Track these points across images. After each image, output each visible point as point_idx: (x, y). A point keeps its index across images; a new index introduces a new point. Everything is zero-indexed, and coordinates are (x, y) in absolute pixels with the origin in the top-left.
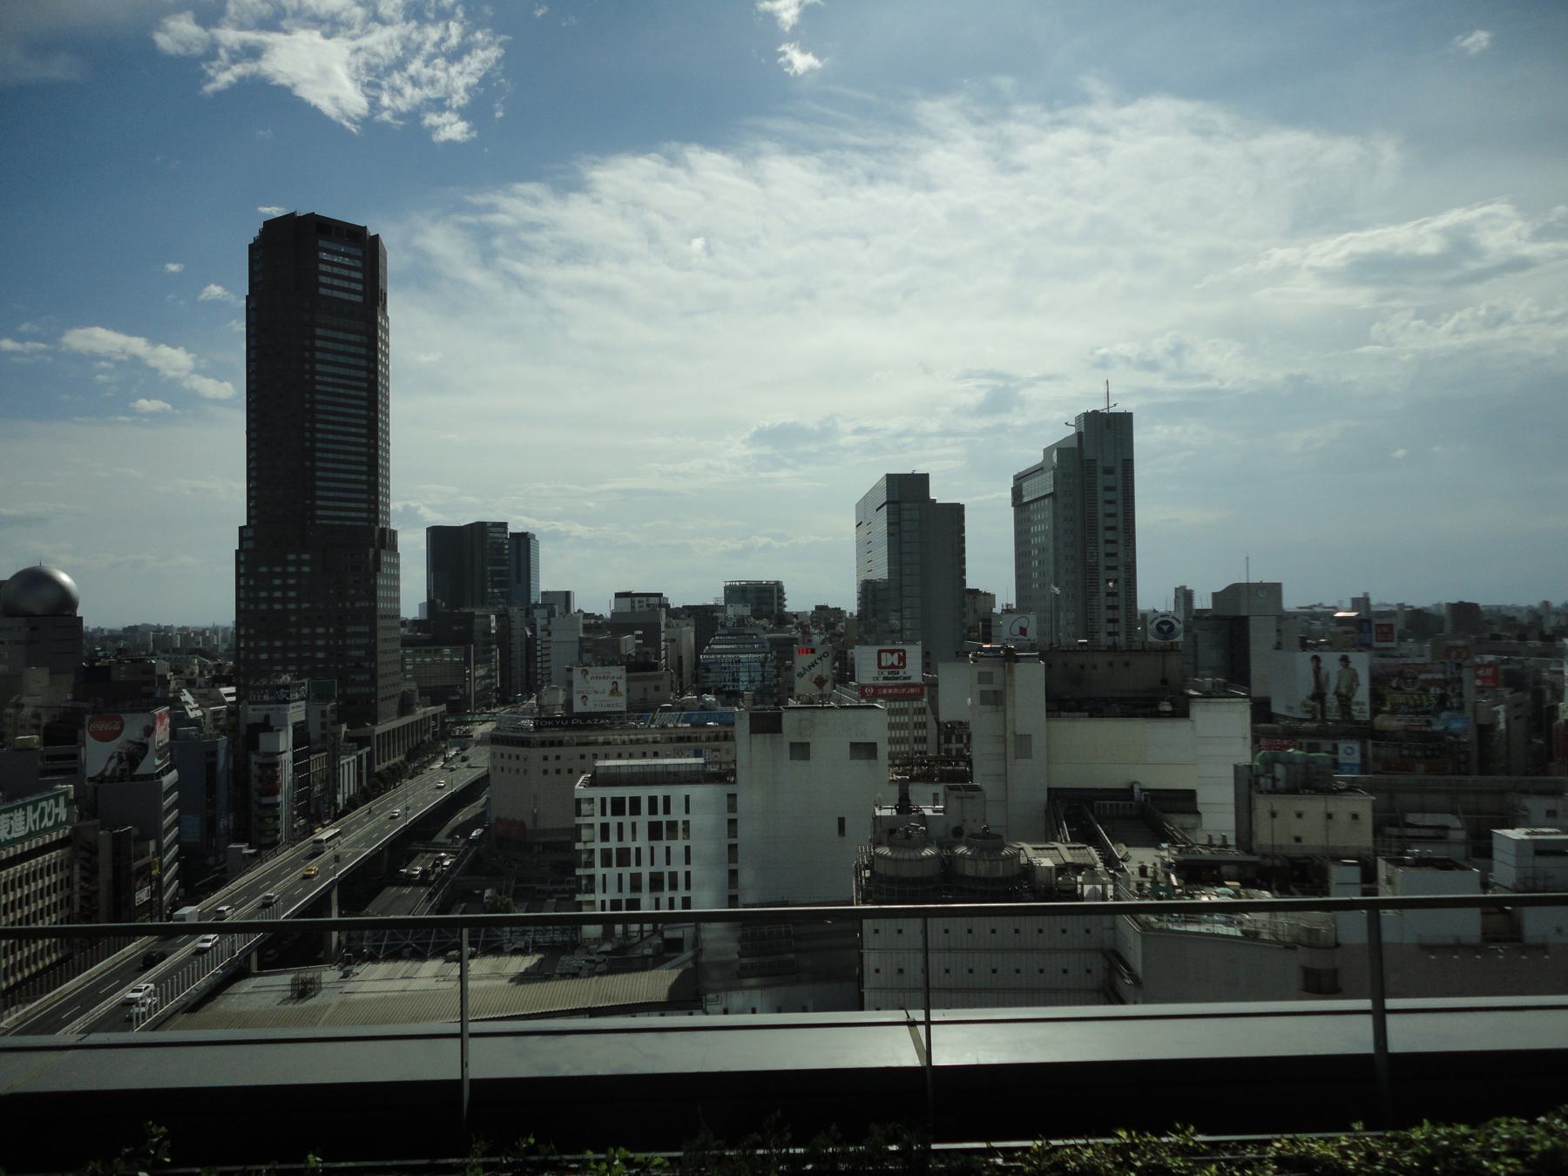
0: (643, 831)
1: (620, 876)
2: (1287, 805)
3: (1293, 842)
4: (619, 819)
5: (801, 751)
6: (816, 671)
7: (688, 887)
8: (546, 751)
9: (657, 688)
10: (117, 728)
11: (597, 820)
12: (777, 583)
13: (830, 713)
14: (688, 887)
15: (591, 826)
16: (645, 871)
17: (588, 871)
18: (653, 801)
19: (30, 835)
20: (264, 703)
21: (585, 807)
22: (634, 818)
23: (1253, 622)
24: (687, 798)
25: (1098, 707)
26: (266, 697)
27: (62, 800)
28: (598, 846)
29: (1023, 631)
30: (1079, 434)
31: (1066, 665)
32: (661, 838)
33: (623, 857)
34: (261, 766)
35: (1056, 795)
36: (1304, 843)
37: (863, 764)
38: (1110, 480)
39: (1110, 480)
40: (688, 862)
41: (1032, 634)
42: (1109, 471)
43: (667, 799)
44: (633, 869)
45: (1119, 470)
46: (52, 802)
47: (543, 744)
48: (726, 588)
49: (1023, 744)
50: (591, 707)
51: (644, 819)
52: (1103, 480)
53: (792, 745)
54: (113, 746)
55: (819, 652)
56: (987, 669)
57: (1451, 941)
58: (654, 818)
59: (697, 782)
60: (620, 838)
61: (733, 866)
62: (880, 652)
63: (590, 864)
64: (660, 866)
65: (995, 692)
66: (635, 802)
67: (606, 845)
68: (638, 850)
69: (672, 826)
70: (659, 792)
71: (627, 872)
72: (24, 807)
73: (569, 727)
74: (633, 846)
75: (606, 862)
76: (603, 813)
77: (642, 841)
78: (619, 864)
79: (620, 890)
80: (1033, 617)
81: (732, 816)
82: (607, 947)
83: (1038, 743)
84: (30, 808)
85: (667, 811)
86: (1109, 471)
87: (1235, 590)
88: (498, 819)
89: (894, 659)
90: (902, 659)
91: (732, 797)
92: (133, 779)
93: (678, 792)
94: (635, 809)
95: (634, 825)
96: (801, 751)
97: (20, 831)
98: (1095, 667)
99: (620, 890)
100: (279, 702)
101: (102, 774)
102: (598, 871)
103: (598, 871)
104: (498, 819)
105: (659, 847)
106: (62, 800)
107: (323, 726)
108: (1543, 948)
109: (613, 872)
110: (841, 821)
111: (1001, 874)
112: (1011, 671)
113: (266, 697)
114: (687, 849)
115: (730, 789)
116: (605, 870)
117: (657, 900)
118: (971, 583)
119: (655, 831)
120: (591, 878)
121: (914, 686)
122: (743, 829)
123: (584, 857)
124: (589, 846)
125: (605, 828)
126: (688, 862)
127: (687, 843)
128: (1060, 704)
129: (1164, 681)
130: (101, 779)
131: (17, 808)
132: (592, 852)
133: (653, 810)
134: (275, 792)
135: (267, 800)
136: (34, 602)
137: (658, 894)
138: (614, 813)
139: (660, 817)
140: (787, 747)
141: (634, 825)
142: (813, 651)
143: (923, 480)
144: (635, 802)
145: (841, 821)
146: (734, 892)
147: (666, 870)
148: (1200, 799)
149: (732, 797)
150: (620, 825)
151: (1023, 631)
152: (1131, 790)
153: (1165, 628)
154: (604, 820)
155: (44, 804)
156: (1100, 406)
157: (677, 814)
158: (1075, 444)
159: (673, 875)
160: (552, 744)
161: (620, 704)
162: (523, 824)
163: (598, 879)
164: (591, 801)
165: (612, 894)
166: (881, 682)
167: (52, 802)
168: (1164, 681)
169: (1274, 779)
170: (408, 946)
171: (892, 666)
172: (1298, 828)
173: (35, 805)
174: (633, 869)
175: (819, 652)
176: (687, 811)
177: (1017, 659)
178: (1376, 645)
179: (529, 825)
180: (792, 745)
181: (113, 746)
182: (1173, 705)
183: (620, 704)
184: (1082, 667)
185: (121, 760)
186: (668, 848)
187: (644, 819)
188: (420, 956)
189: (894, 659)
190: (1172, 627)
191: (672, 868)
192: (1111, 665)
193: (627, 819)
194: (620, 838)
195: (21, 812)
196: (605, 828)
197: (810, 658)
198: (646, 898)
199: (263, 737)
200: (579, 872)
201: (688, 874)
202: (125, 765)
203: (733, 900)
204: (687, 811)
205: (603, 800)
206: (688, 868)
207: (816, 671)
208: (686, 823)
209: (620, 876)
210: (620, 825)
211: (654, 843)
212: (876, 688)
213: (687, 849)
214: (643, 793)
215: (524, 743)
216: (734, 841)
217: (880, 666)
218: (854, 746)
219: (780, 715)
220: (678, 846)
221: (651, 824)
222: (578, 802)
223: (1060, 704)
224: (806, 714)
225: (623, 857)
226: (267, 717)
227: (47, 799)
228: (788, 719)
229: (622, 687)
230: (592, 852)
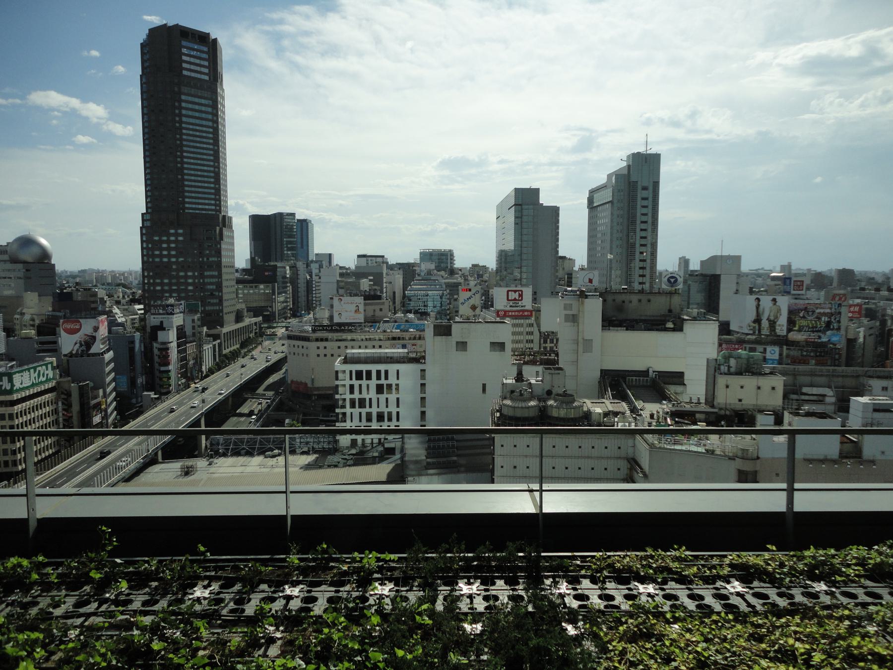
0: (373, 389)
1: (360, 413)
2: (736, 381)
3: (737, 402)
4: (360, 382)
5: (462, 346)
6: (472, 302)
7: (398, 420)
8: (319, 344)
9: (381, 310)
10: (77, 327)
11: (348, 382)
12: (450, 251)
13: (479, 325)
14: (398, 420)
15: (344, 386)
16: (374, 410)
17: (343, 410)
18: (378, 372)
19: (33, 385)
20: (160, 314)
21: (340, 375)
22: (369, 382)
23: (722, 277)
24: (398, 371)
25: (632, 325)
26: (161, 311)
27: (50, 366)
28: (348, 396)
29: (591, 281)
30: (629, 166)
31: (614, 300)
32: (383, 393)
33: (362, 403)
34: (159, 349)
35: (605, 373)
36: (743, 402)
37: (497, 354)
38: (645, 194)
39: (645, 194)
40: (398, 406)
41: (596, 283)
42: (645, 188)
43: (386, 372)
44: (368, 409)
45: (651, 188)
46: (44, 367)
47: (317, 340)
48: (421, 253)
49: (588, 344)
50: (343, 320)
51: (374, 382)
52: (641, 194)
54: (77, 337)
55: (473, 291)
56: (568, 302)
57: (822, 457)
58: (379, 382)
59: (404, 362)
60: (360, 393)
61: (423, 409)
62: (508, 291)
63: (344, 407)
64: (383, 408)
65: (573, 315)
66: (369, 373)
67: (352, 396)
68: (370, 399)
69: (389, 386)
70: (382, 367)
71: (364, 411)
72: (29, 370)
73: (332, 331)
74: (367, 397)
75: (353, 405)
76: (351, 379)
77: (373, 394)
78: (360, 407)
80: (596, 273)
81: (423, 382)
82: (353, 451)
83: (596, 345)
84: (32, 371)
85: (386, 378)
86: (645, 188)
87: (714, 260)
88: (292, 381)
89: (516, 295)
90: (521, 295)
91: (423, 371)
92: (89, 355)
93: (392, 368)
94: (369, 377)
95: (368, 386)
96: (462, 346)
97: (27, 383)
98: (631, 302)
99: (360, 421)
100: (168, 314)
101: (71, 353)
102: (348, 410)
103: (348, 410)
104: (292, 381)
105: (383, 397)
106: (50, 366)
107: (194, 328)
108: (873, 462)
109: (356, 411)
110: (484, 386)
112: (583, 303)
113: (161, 311)
114: (398, 399)
116: (352, 410)
118: (561, 253)
119: (380, 389)
120: (344, 414)
121: (527, 311)
122: (428, 388)
123: (340, 403)
124: (343, 397)
125: (352, 387)
126: (398, 406)
128: (610, 322)
129: (670, 311)
130: (71, 355)
131: (25, 370)
132: (344, 400)
133: (379, 378)
134: (167, 364)
135: (163, 369)
136: (28, 255)
138: (357, 379)
139: (383, 381)
141: (368, 386)
142: (470, 290)
143: (535, 192)
144: (369, 373)
145: (484, 386)
147: (386, 411)
148: (686, 377)
150: (360, 386)
151: (591, 281)
152: (648, 371)
153: (672, 280)
154: (351, 382)
155: (40, 368)
156: (641, 149)
157: (392, 380)
158: (626, 172)
159: (390, 414)
160: (322, 340)
161: (360, 318)
162: (306, 384)
163: (348, 415)
164: (344, 372)
166: (508, 308)
167: (44, 367)
168: (670, 311)
169: (729, 367)
170: (244, 449)
171: (515, 299)
172: (741, 394)
173: (35, 368)
174: (368, 409)
175: (473, 291)
176: (398, 378)
177: (586, 297)
178: (793, 292)
179: (310, 385)
181: (77, 337)
182: (674, 324)
183: (360, 318)
185: (81, 345)
186: (387, 399)
187: (374, 382)
188: (250, 454)
189: (516, 295)
190: (676, 280)
191: (389, 410)
192: (640, 301)
193: (364, 382)
194: (360, 393)
195: (27, 373)
196: (352, 387)
197: (468, 294)
199: (159, 333)
200: (337, 411)
201: (398, 413)
202: (84, 348)
204: (398, 378)
205: (351, 372)
206: (398, 410)
207: (472, 302)
208: (397, 385)
209: (360, 413)
210: (360, 386)
211: (379, 396)
212: (505, 312)
213: (398, 399)
214: (374, 368)
215: (306, 339)
216: (423, 395)
217: (508, 299)
218: (492, 344)
219: (451, 326)
220: (392, 397)
221: (377, 385)
222: (337, 372)
223: (610, 322)
225: (362, 403)
226: (162, 322)
227: (41, 366)
228: (455, 328)
229: (361, 308)
230: (344, 400)
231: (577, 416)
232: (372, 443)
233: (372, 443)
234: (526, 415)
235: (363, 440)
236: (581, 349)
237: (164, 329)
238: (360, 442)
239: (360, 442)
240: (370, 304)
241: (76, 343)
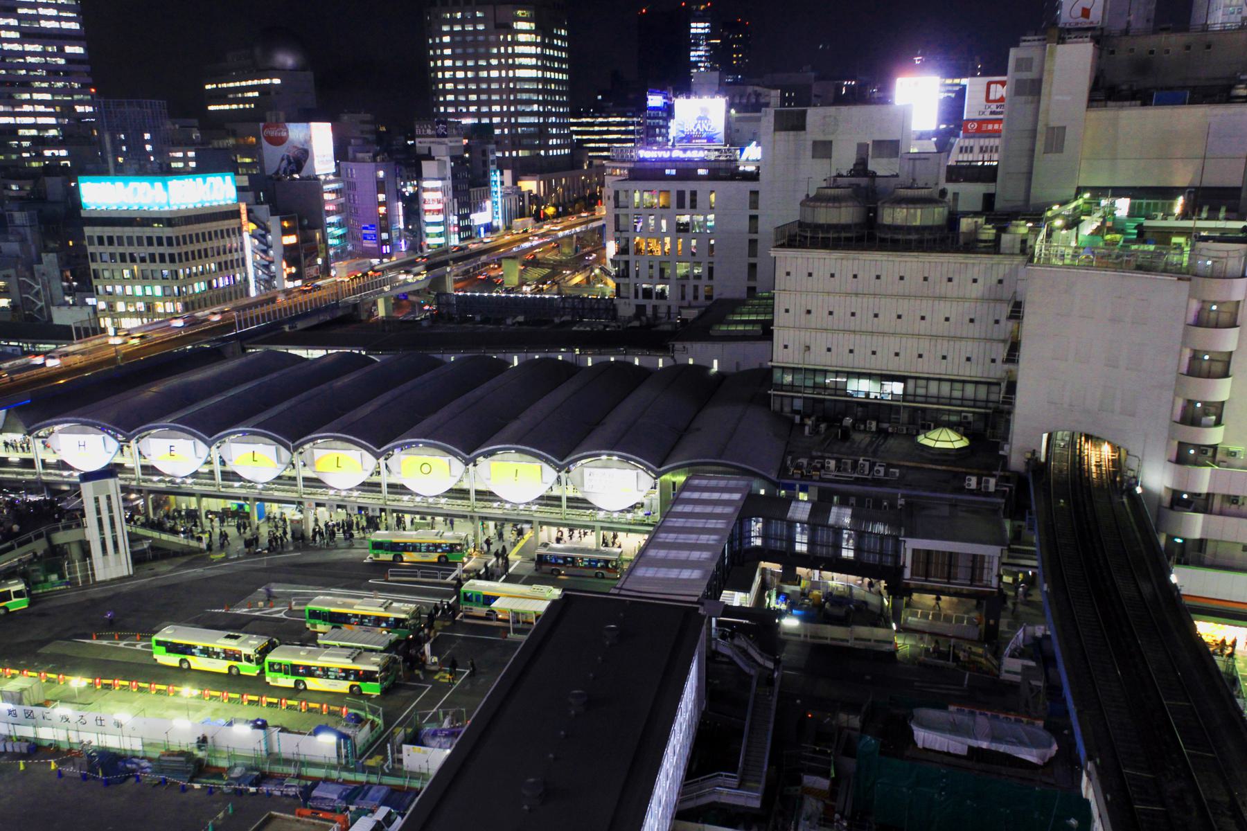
26: (429, 132)
43: (694, 194)
53: (815, 143)
61: (752, 260)
62: (989, 84)
65: (1033, 81)
81: (754, 212)
82: (636, 323)
91: (755, 193)
100: (438, 136)
111: (918, 223)
113: (429, 132)
128: (1105, 91)
146: (752, 284)
180: (815, 143)
184: (1152, 52)
185: (289, 163)
202: (293, 166)
203: (752, 290)
216: (754, 236)
217: (988, 100)
223: (1105, 91)
231: (929, 223)
232: (669, 312)
233: (669, 312)
234: (835, 221)
235: (655, 308)
236: (1040, 146)
237: (432, 159)
238: (649, 312)
239: (649, 312)
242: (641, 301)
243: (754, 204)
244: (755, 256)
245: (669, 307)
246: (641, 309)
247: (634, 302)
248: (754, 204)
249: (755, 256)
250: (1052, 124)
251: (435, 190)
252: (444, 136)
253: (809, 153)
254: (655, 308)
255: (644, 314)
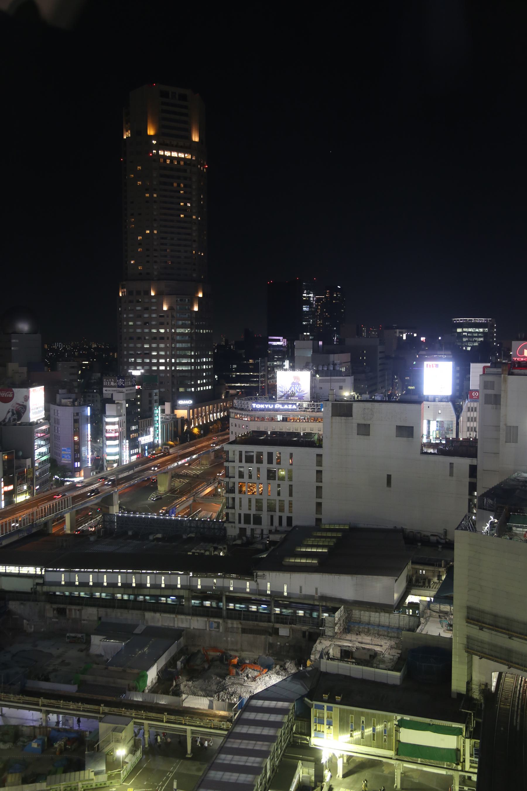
5: (364, 429)
7: (290, 511)
10: (11, 396)
13: (377, 405)
14: (290, 511)
18: (270, 455)
20: (111, 387)
26: (112, 384)
51: (265, 466)
61: (319, 500)
65: (496, 396)
79: (250, 509)
81: (319, 468)
82: (239, 542)
91: (319, 456)
99: (250, 509)
100: (119, 387)
110: (389, 477)
112: (505, 380)
113: (112, 384)
114: (291, 486)
115: (318, 451)
117: (272, 517)
122: (324, 474)
126: (291, 495)
127: (291, 483)
133: (270, 461)
137: (272, 513)
138: (246, 462)
140: (355, 426)
145: (389, 477)
146: (319, 516)
149: (319, 456)
165: (245, 510)
185: (13, 414)
187: (265, 466)
191: (281, 498)
198: (265, 516)
201: (290, 503)
202: (15, 417)
203: (318, 520)
205: (241, 453)
213: (291, 486)
214: (265, 449)
216: (320, 484)
224: (368, 405)
230: (234, 483)
235: (252, 530)
238: (249, 533)
240: (327, 381)
241: (9, 412)
242: (243, 525)
243: (319, 463)
244: (321, 498)
245: (262, 530)
246: (243, 531)
247: (238, 526)
248: (319, 463)
249: (321, 498)
250: (509, 425)
251: (113, 424)
252: (122, 387)
253: (355, 431)
254: (252, 530)
255: (245, 535)
